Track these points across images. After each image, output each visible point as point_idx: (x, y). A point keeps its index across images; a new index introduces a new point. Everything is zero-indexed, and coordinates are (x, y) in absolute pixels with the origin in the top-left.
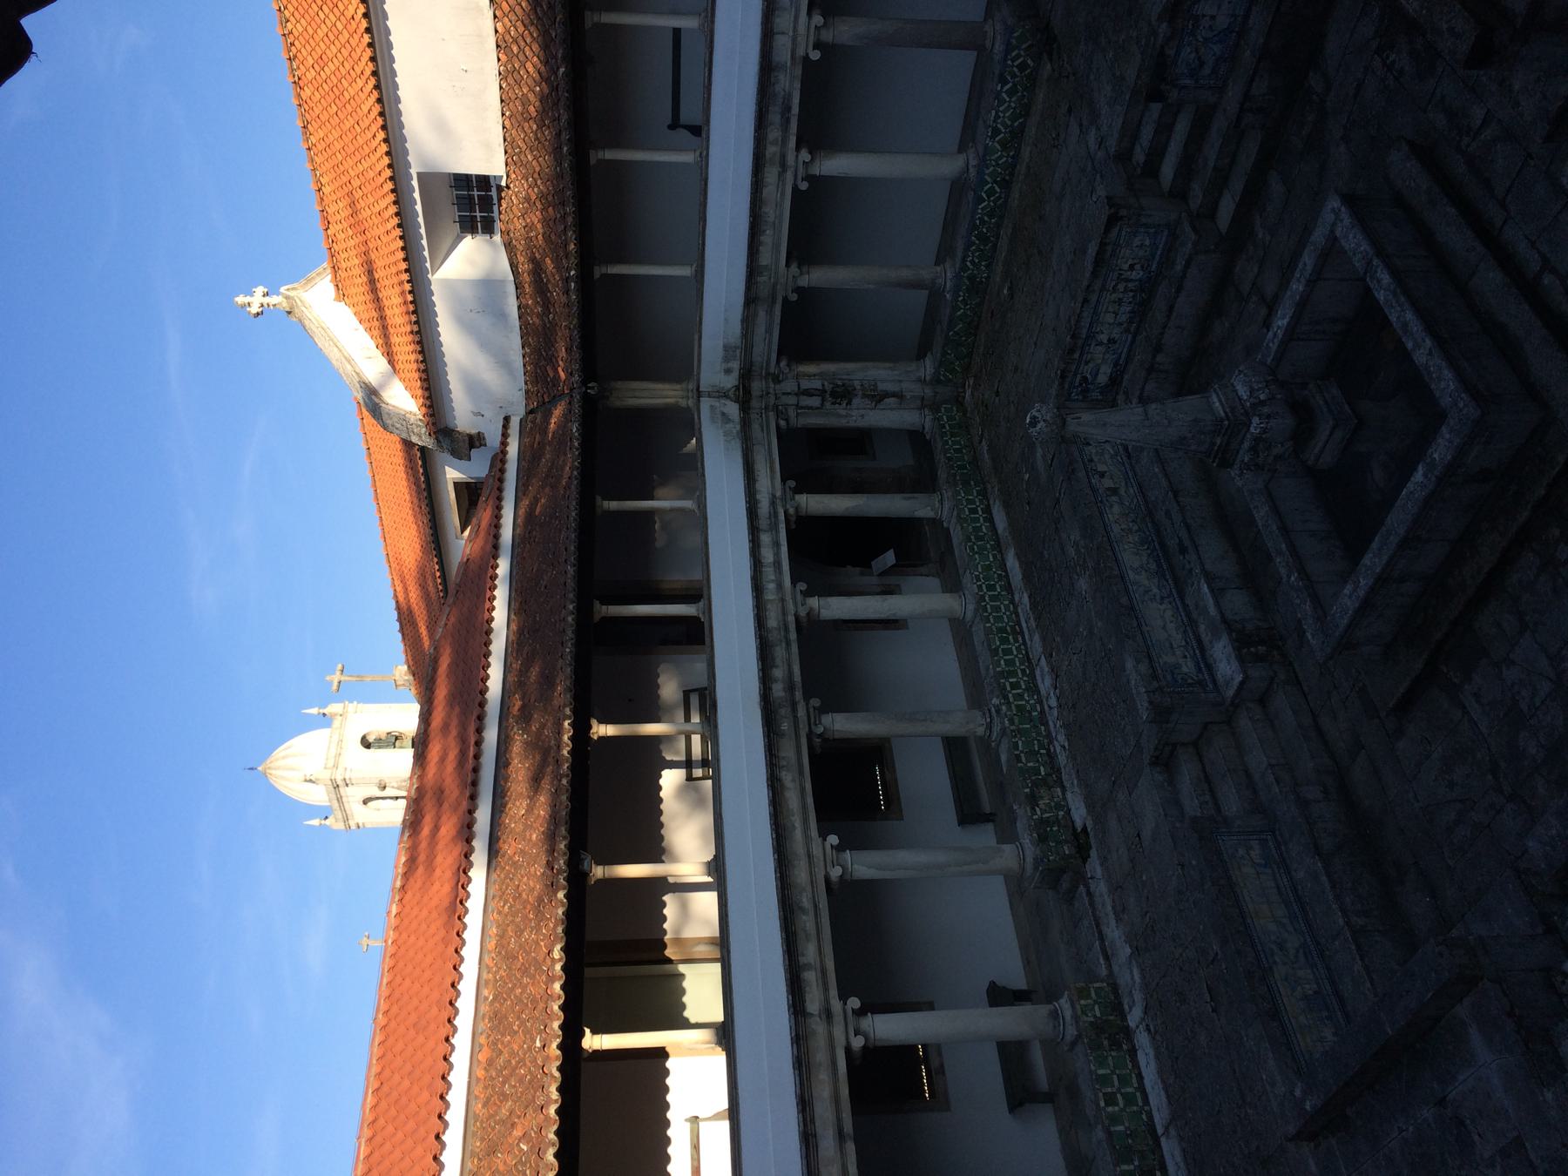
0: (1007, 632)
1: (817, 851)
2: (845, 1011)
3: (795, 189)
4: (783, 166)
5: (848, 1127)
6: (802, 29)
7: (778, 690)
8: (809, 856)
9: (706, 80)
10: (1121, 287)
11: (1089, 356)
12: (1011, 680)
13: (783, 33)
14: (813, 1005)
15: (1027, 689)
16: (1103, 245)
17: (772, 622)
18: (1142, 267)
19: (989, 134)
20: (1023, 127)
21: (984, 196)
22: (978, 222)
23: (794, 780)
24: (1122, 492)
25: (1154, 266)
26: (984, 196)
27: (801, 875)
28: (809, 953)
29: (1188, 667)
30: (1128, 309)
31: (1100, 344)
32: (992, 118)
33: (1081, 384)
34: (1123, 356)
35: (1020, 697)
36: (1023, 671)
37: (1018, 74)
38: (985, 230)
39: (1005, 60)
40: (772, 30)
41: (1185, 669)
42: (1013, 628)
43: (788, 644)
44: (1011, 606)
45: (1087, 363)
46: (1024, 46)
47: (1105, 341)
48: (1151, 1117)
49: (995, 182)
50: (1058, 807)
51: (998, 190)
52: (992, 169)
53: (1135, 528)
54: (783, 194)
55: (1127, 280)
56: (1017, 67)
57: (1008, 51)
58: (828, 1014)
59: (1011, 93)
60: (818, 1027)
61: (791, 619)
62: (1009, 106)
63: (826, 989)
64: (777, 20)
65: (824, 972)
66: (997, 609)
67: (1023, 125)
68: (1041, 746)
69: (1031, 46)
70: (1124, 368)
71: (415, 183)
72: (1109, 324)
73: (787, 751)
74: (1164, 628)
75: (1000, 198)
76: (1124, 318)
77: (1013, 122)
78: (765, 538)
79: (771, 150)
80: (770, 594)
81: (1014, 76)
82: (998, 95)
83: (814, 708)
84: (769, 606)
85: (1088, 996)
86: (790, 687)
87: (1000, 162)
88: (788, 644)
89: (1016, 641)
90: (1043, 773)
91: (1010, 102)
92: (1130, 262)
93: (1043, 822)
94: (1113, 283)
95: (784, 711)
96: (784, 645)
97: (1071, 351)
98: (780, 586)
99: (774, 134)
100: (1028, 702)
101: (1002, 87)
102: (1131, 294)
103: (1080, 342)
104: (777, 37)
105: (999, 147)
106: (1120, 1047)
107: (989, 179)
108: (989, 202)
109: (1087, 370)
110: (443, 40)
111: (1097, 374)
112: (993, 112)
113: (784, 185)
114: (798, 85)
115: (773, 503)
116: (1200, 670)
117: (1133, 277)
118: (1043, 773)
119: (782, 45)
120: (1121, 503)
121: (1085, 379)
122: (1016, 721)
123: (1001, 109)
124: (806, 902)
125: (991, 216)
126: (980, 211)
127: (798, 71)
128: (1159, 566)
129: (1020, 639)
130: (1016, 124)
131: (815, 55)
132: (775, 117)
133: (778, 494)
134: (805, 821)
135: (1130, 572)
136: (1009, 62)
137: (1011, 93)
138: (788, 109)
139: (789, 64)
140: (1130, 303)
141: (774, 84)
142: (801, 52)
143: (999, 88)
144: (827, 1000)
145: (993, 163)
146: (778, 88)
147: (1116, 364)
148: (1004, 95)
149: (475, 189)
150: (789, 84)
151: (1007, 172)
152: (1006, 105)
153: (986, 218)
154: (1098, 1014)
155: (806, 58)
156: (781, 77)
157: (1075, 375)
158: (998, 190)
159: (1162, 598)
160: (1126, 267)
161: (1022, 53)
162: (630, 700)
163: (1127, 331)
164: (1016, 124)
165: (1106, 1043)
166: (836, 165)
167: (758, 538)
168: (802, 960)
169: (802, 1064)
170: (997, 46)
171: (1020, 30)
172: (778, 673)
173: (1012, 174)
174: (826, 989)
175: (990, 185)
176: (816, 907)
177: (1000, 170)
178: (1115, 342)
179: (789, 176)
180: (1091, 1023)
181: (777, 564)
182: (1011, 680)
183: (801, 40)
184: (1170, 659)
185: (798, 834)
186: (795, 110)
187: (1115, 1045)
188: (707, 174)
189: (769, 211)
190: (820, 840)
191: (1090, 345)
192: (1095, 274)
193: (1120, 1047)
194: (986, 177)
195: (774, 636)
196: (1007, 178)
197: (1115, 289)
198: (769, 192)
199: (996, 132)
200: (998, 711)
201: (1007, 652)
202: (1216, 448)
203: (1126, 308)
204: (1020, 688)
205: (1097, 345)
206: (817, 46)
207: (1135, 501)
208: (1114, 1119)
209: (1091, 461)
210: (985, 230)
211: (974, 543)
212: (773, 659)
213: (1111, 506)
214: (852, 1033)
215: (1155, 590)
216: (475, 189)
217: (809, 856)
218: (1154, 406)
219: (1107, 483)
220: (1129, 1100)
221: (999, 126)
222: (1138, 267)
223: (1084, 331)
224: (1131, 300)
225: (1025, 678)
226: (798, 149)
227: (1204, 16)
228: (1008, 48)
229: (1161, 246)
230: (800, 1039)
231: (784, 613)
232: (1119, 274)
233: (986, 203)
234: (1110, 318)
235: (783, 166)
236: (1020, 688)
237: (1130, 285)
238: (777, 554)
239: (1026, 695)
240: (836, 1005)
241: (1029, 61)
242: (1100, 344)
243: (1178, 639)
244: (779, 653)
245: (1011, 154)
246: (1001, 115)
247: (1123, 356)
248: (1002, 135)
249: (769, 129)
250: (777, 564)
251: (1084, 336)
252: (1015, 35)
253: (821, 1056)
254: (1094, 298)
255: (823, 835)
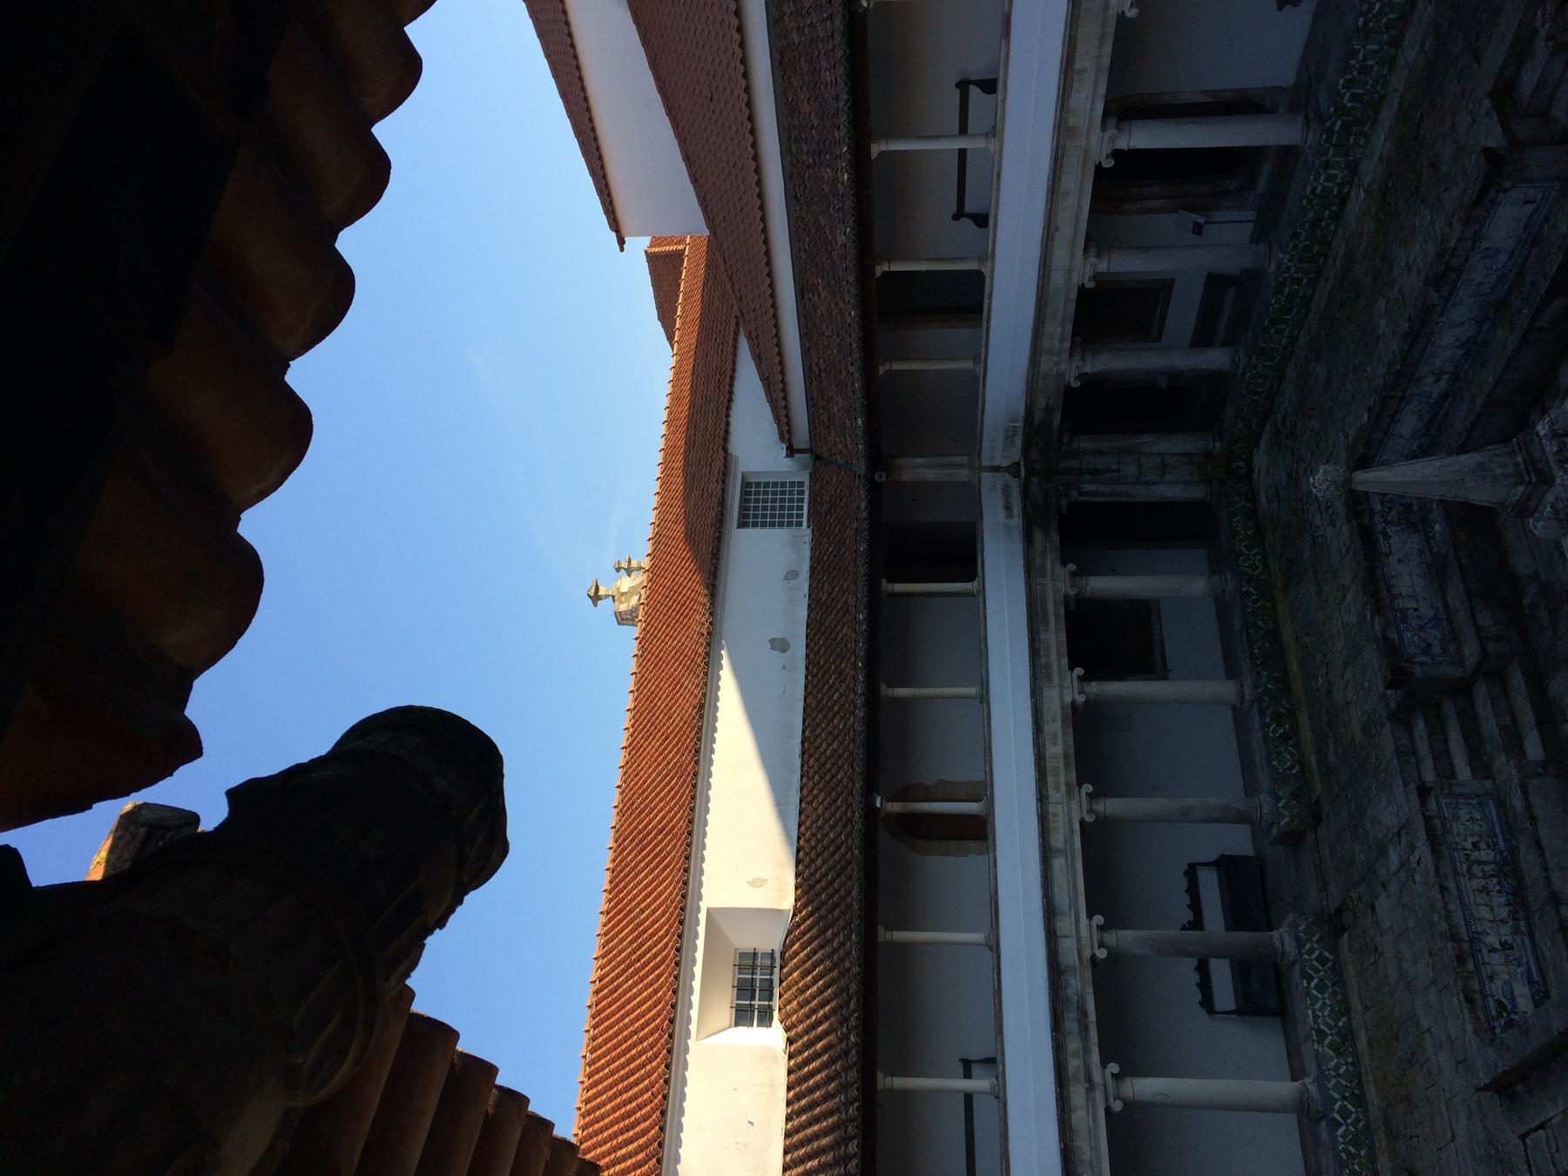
3: (1108, 1111)
4: (1089, 1079)
6: (1084, 932)
9: (996, 984)
10: (1476, 869)
11: (1488, 967)
13: (1067, 937)
16: (1427, 819)
18: (1488, 845)
19: (1315, 1038)
20: (1348, 1025)
21: (1338, 1117)
22: (1343, 1155)
25: (1502, 844)
26: (1338, 1117)
30: (1502, 900)
31: (1492, 950)
32: (1312, 1020)
33: (1500, 1014)
34: (1533, 968)
37: (1320, 967)
38: (1356, 1167)
39: (1301, 954)
40: (1055, 933)
45: (1491, 979)
46: (1314, 939)
47: (1498, 946)
49: (1344, 1098)
51: (1353, 1110)
52: (1333, 1081)
54: (1095, 1118)
55: (1479, 863)
56: (1316, 960)
57: (1299, 949)
59: (1321, 988)
62: (1324, 1003)
64: (1059, 924)
67: (1348, 1025)
69: (1322, 938)
70: (1545, 986)
71: (702, 917)
72: (1491, 921)
75: (1357, 1120)
76: (1503, 912)
77: (1337, 1021)
79: (1074, 1064)
81: (1317, 971)
82: (1308, 993)
87: (1342, 1071)
91: (1311, 960)
92: (1470, 840)
94: (1465, 866)
97: (1460, 959)
99: (1073, 1044)
101: (1309, 983)
102: (1495, 880)
103: (1466, 946)
104: (1062, 940)
105: (1332, 1053)
107: (1336, 1096)
108: (1347, 1125)
109: (1496, 988)
110: (736, 1090)
111: (1513, 999)
112: (1310, 1012)
113: (1094, 1106)
114: (1090, 989)
117: (1483, 858)
119: (1068, 947)
121: (1499, 1003)
123: (1317, 1007)
125: (1357, 1145)
126: (1340, 1139)
127: (1088, 974)
130: (1340, 1024)
131: (1102, 954)
132: (1071, 1025)
136: (1306, 956)
137: (1321, 988)
138: (1085, 1014)
139: (1077, 963)
140: (1499, 892)
141: (1065, 988)
142: (1087, 955)
143: (1305, 985)
145: (1332, 1073)
146: (1070, 992)
147: (1531, 982)
148: (1315, 992)
149: (756, 1007)
150: (1080, 985)
151: (1354, 1084)
152: (1320, 1003)
153: (1353, 1150)
155: (1093, 957)
156: (1072, 981)
157: (1485, 997)
158: (1353, 1110)
160: (1469, 846)
161: (1315, 945)
163: (1516, 931)
164: (1340, 1024)
166: (1145, 1087)
170: (1287, 944)
171: (1305, 923)
173: (1361, 1086)
175: (1340, 1103)
177: (1344, 1082)
178: (1511, 948)
179: (1099, 1096)
183: (1086, 942)
186: (1092, 1017)
188: (990, 744)
189: (1082, 1144)
191: (1480, 951)
192: (1436, 853)
194: (1331, 1092)
196: (1356, 1091)
197: (1472, 876)
198: (1079, 1117)
199: (1321, 1035)
202: (1522, 466)
203: (1499, 900)
205: (1489, 952)
206: (1101, 945)
210: (1356, 1167)
216: (756, 1007)
221: (1321, 1026)
222: (1482, 845)
223: (1463, 930)
224: (1498, 888)
226: (1104, 1064)
227: (1408, 609)
228: (1300, 945)
229: (1495, 819)
232: (1466, 855)
233: (1343, 1128)
234: (1484, 912)
235: (1091, 1089)
237: (1487, 868)
241: (1326, 954)
242: (1492, 950)
245: (1350, 1060)
246: (1320, 1014)
247: (1533, 968)
248: (1330, 1037)
249: (1068, 1039)
251: (1466, 938)
252: (1301, 928)
254: (1452, 885)
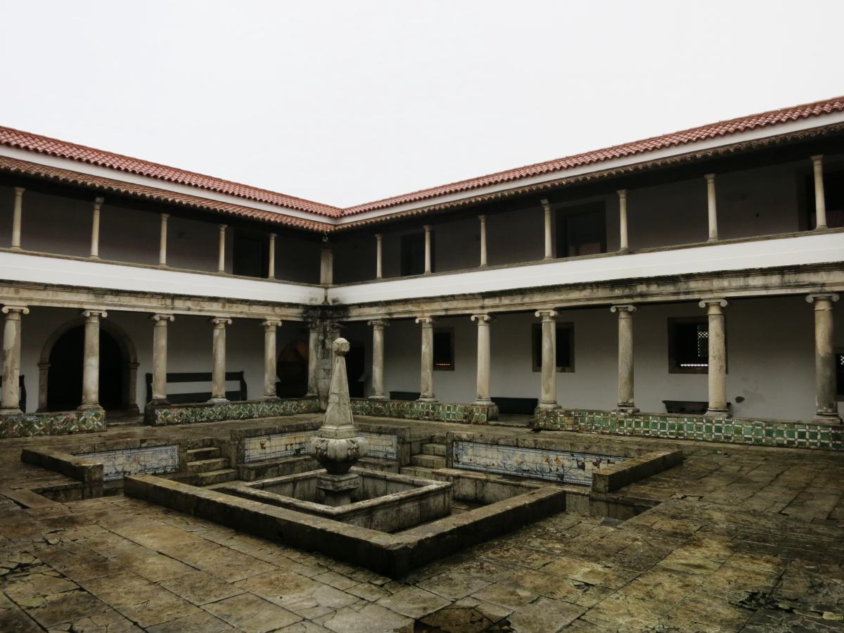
0: (678, 430)
1: (549, 306)
2: (483, 314)
5: (450, 313)
7: (642, 288)
8: (545, 302)
12: (642, 423)
14: (488, 302)
15: (634, 430)
17: (693, 285)
23: (585, 296)
24: (580, 471)
27: (538, 298)
28: (506, 301)
29: (465, 459)
35: (630, 426)
36: (648, 432)
41: (464, 457)
42: (680, 434)
43: (674, 294)
44: (701, 439)
48: (443, 421)
50: (562, 426)
53: (552, 469)
58: (483, 307)
60: (480, 303)
61: (696, 296)
63: (492, 307)
65: (497, 306)
66: (699, 429)
68: (596, 428)
73: (601, 293)
74: (486, 457)
78: (775, 280)
80: (717, 283)
83: (627, 308)
84: (707, 282)
85: (482, 412)
86: (642, 295)
88: (674, 294)
89: (671, 434)
90: (581, 424)
93: (556, 416)
95: (627, 292)
96: (676, 291)
98: (723, 290)
100: (626, 428)
106: (464, 418)
115: (813, 285)
116: (463, 464)
118: (581, 424)
120: (570, 468)
122: (613, 418)
124: (527, 300)
128: (525, 471)
129: (672, 437)
133: (827, 289)
134: (562, 301)
135: (520, 453)
144: (488, 307)
154: (476, 414)
159: (505, 464)
162: (757, 215)
165: (466, 414)
167: (774, 274)
168: (503, 298)
169: (465, 297)
172: (654, 288)
174: (492, 307)
176: (523, 304)
180: (473, 410)
181: (746, 288)
182: (642, 423)
184: (470, 451)
185: (557, 297)
187: (465, 417)
190: (553, 307)
193: (464, 418)
195: (682, 286)
200: (622, 411)
201: (663, 426)
204: (636, 427)
207: (574, 477)
208: (443, 408)
209: (609, 462)
211: (763, 428)
212: (663, 285)
213: (569, 460)
214: (476, 316)
215: (509, 462)
217: (545, 302)
218: (337, 399)
219: (589, 466)
220: (448, 415)
225: (642, 432)
230: (472, 296)
231: (700, 292)
236: (636, 427)
238: (755, 288)
239: (630, 428)
240: (486, 311)
243: (482, 461)
244: (670, 289)
250: (746, 288)
253: (470, 304)
255: (555, 309)
